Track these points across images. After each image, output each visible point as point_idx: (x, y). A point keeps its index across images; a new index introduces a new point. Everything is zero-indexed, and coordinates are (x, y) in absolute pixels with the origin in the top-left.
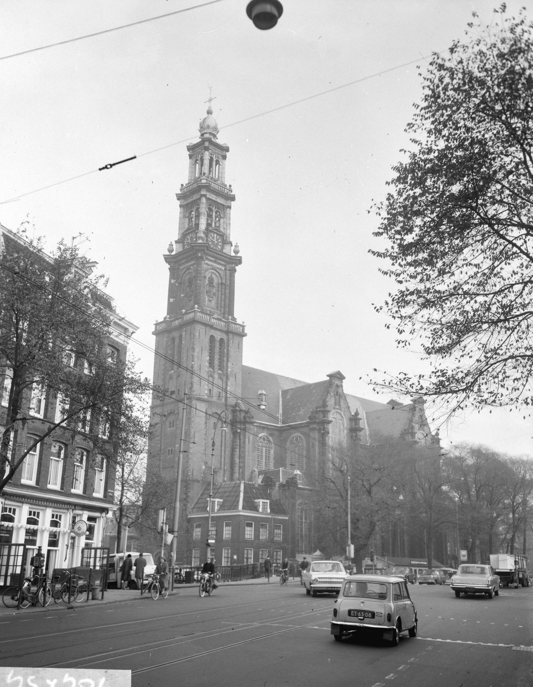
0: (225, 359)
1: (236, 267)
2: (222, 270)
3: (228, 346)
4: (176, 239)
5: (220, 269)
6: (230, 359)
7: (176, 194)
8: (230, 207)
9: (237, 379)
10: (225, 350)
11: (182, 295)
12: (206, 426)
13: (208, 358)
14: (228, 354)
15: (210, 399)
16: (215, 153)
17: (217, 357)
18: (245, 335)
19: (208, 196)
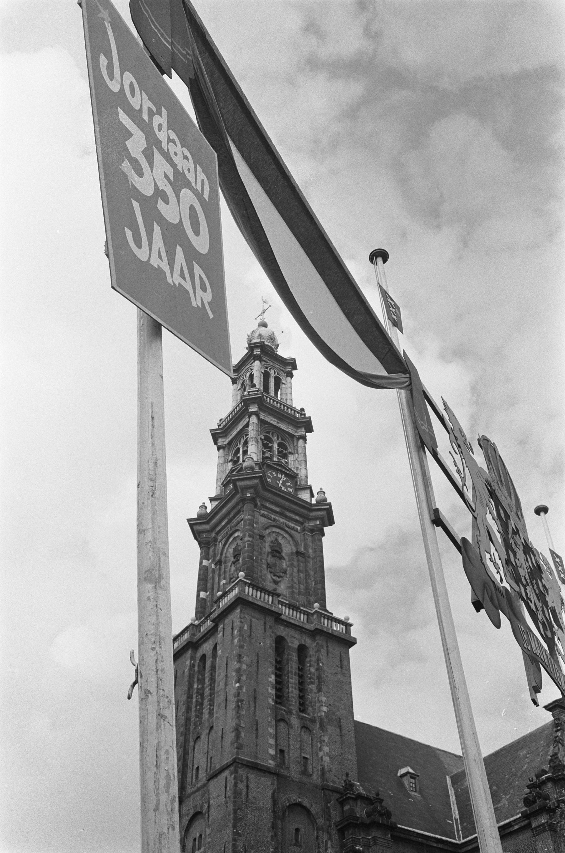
0: (313, 687)
1: (325, 528)
2: (297, 531)
3: (318, 660)
4: (213, 495)
5: (293, 529)
6: (324, 688)
7: (211, 430)
8: (304, 438)
9: (344, 732)
10: (313, 670)
11: (224, 582)
12: (276, 835)
13: (272, 678)
14: (319, 678)
15: (284, 772)
16: (273, 368)
17: (293, 681)
18: (352, 643)
19: (262, 417)
